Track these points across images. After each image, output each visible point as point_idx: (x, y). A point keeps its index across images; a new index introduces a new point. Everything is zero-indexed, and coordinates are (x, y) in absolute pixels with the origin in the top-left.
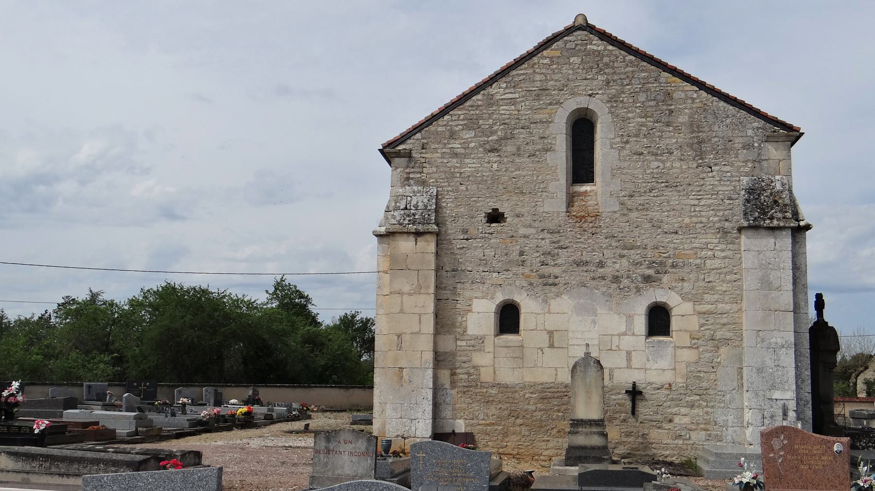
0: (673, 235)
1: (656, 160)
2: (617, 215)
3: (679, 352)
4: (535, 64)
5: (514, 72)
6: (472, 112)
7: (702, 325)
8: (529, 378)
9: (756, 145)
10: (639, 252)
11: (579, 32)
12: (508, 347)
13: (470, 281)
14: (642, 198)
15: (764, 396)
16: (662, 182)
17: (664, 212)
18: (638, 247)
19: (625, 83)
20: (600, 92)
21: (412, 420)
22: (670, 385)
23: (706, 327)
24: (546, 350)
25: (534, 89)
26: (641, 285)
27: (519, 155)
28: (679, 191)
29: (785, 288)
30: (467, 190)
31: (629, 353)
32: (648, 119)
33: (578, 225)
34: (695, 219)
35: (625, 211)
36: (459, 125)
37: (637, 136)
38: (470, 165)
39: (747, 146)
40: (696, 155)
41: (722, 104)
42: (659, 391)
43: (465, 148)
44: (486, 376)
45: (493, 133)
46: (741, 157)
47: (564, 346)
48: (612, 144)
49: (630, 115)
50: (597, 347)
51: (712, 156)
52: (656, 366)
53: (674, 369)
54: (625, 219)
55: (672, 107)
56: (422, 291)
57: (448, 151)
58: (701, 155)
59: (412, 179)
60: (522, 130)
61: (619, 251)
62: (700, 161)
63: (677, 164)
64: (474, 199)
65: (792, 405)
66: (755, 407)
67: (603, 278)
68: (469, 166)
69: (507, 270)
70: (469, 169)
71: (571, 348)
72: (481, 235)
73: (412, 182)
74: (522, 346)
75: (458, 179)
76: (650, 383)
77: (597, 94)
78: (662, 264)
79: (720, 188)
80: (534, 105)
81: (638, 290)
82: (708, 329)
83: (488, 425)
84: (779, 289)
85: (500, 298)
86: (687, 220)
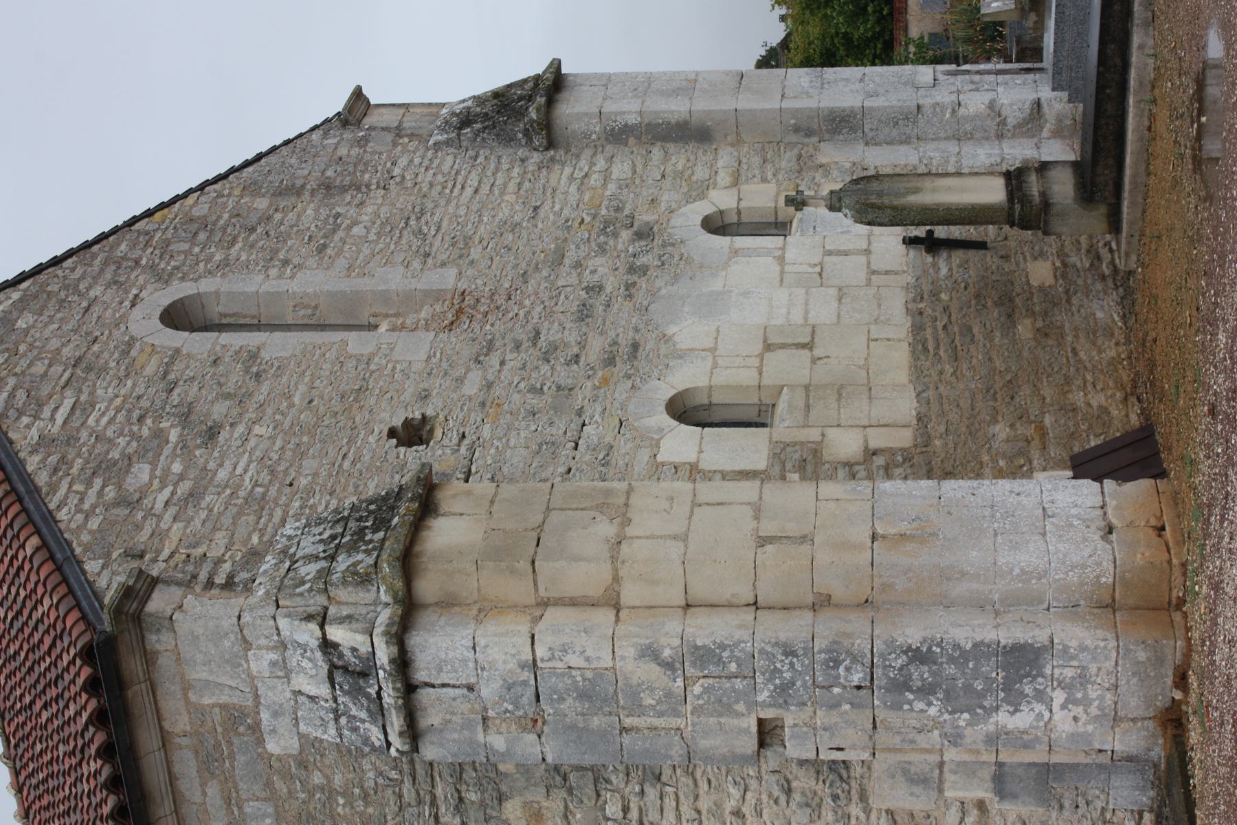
1: (349, 228)
7: (764, 180)
10: (573, 247)
12: (808, 407)
24: (818, 352)
25: (67, 375)
31: (830, 253)
34: (512, 187)
38: (239, 471)
41: (250, 169)
47: (809, 329)
57: (173, 510)
61: (564, 270)
62: (374, 187)
69: (580, 413)
70: (250, 474)
71: (811, 321)
72: (463, 450)
75: (273, 491)
78: (607, 223)
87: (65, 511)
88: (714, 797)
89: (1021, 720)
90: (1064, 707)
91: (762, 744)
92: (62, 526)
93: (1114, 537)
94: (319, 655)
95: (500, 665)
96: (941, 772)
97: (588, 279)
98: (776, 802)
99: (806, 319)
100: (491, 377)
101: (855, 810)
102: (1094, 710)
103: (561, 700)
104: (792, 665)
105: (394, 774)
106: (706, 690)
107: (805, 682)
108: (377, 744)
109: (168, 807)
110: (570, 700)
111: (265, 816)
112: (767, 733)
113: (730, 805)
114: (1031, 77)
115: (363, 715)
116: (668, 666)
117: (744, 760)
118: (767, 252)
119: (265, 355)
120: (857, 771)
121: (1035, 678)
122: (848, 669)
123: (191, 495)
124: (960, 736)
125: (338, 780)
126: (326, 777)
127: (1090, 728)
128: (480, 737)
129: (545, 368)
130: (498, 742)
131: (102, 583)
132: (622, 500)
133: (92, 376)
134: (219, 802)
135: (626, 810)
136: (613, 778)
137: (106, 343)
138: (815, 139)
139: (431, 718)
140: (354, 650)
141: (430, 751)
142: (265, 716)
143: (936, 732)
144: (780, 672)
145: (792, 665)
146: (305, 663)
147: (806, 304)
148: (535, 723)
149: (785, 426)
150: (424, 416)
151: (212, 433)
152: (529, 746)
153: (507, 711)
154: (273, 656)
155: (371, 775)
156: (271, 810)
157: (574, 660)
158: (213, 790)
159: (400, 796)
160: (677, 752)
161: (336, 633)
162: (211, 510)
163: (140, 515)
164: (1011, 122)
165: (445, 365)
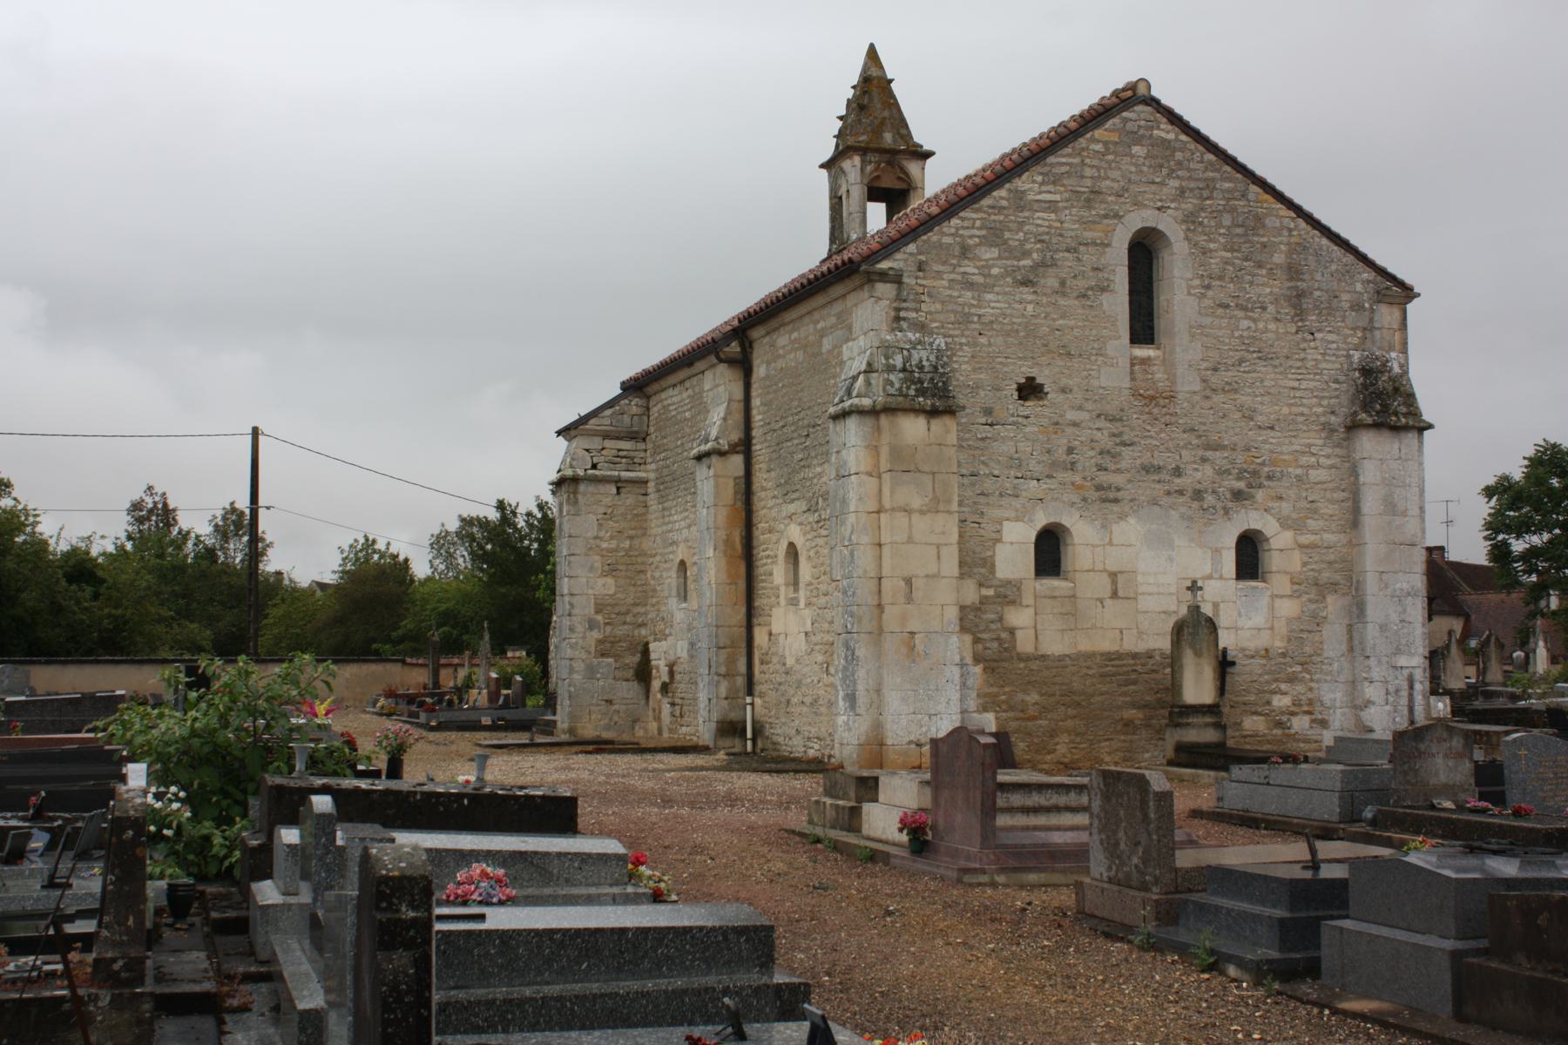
0: (1269, 431)
1: (1247, 318)
2: (1197, 398)
3: (1278, 602)
4: (1083, 149)
5: (1051, 159)
6: (993, 217)
7: (1305, 564)
8: (1085, 646)
9: (1367, 305)
10: (1226, 455)
11: (1140, 108)
12: (1055, 597)
13: (997, 493)
14: (1230, 374)
15: (1388, 663)
16: (1254, 352)
17: (1256, 396)
18: (1224, 448)
19: (1205, 196)
20: (1173, 205)
21: (930, 716)
22: (1267, 650)
23: (1310, 567)
24: (1108, 602)
25: (1083, 189)
26: (1230, 504)
27: (1064, 295)
28: (1275, 367)
29: (1410, 513)
30: (990, 345)
32: (1235, 254)
33: (1147, 410)
34: (1295, 410)
35: (1208, 393)
36: (974, 236)
37: (1221, 278)
38: (992, 305)
39: (1357, 307)
40: (1296, 315)
41: (1325, 241)
42: (1252, 660)
43: (984, 276)
44: (1025, 644)
45: (1026, 254)
46: (1349, 322)
47: (1132, 595)
48: (1190, 287)
49: (1212, 246)
50: (1175, 598)
51: (1314, 318)
52: (1250, 624)
53: (1272, 628)
54: (1207, 404)
55: (1265, 239)
56: (941, 507)
58: (1300, 314)
59: (904, 319)
60: (1066, 254)
61: (1200, 453)
62: (1300, 324)
63: (1272, 326)
64: (1000, 360)
65: (1419, 675)
66: (1377, 678)
67: (1181, 493)
68: (992, 305)
70: (991, 311)
72: (1012, 419)
73: (904, 325)
74: (1074, 596)
76: (1243, 650)
77: (1169, 207)
78: (1255, 473)
79: (1324, 365)
80: (1083, 217)
81: (1226, 511)
82: (1312, 570)
84: (1404, 513)
85: (1041, 520)
86: (1285, 410)
87: (958, 221)
92: (946, 224)
99: (1143, 594)
109: (828, 299)
131: (898, 256)
137: (1116, 203)
138: (1354, 593)
147: (1159, 594)
150: (1047, 393)
151: (1026, 283)
162: (959, 297)
163: (954, 262)
164: (1362, 714)
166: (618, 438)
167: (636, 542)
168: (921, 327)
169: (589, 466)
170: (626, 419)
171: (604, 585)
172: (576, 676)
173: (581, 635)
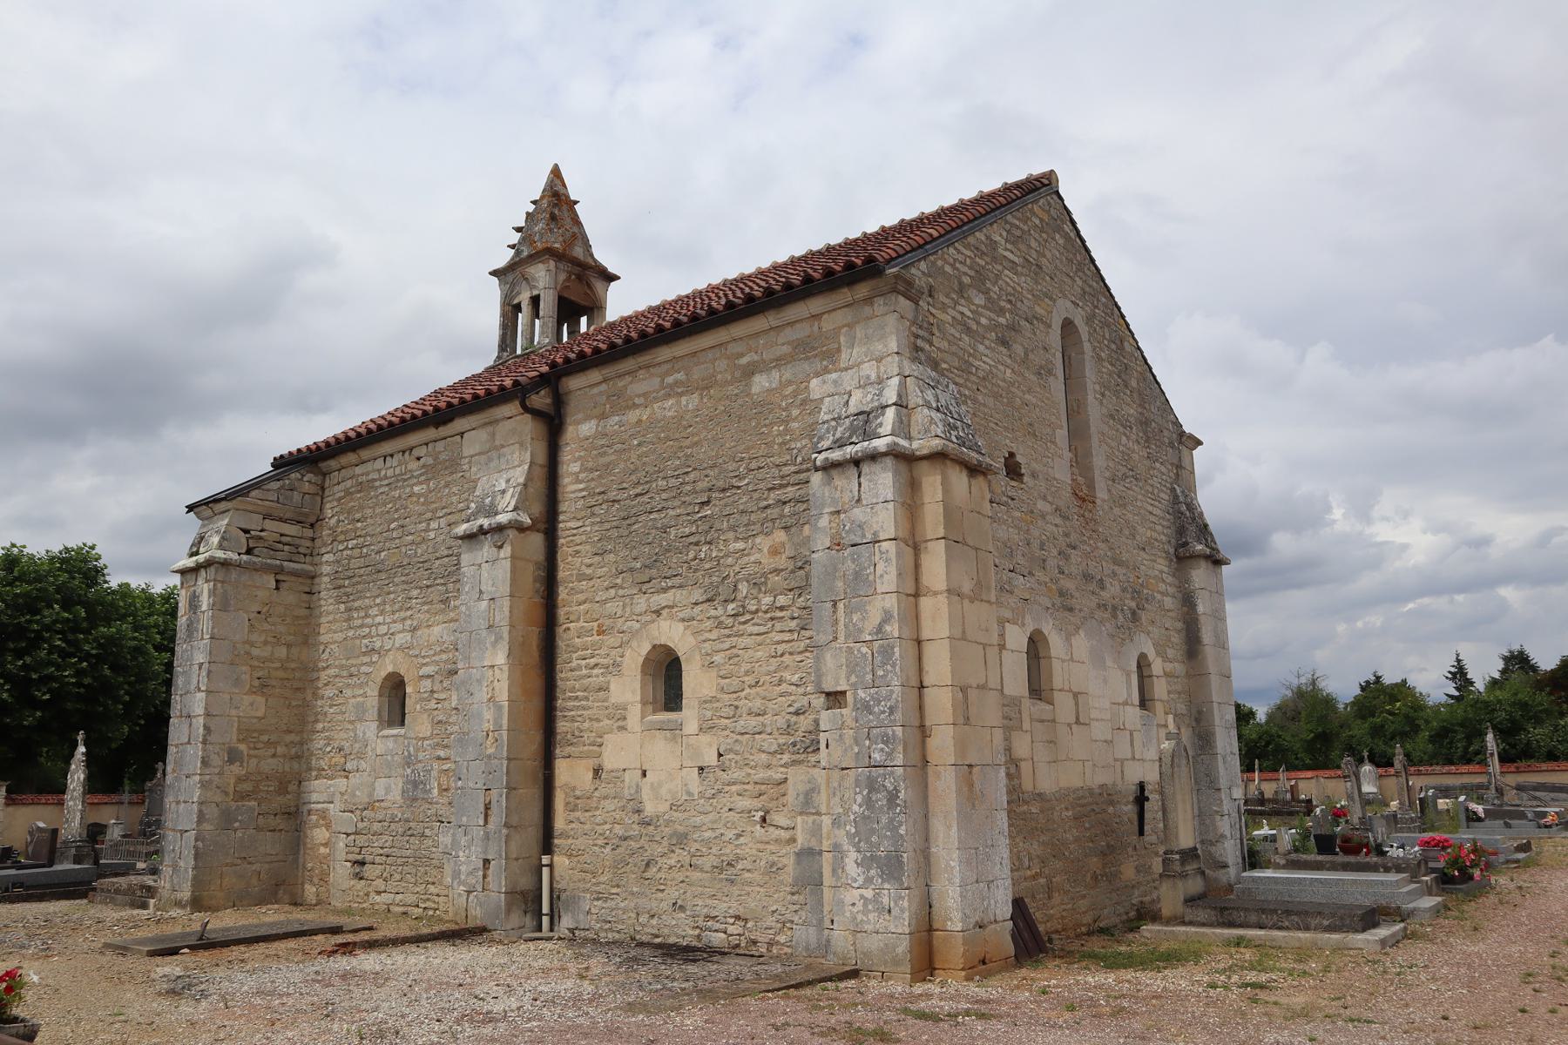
1: (1125, 434)
7: (1169, 692)
12: (1042, 721)
24: (1074, 727)
31: (1131, 735)
34: (1155, 535)
38: (984, 358)
57: (959, 317)
69: (1030, 573)
72: (1005, 499)
75: (974, 378)
83: (1034, 877)
88: (791, 664)
89: (852, 869)
90: (862, 897)
91: (828, 694)
93: (978, 930)
94: (876, 404)
95: (875, 519)
96: (813, 814)
97: (1107, 581)
98: (790, 706)
100: (1048, 517)
101: (786, 758)
102: (860, 917)
103: (853, 561)
104: (884, 712)
105: (799, 459)
106: (864, 655)
107: (871, 721)
108: (819, 445)
109: (774, 323)
110: (853, 566)
111: (771, 382)
112: (835, 698)
113: (787, 675)
114: (1240, 860)
115: (838, 435)
116: (879, 629)
117: (818, 683)
118: (1129, 695)
119: (1051, 379)
120: (813, 758)
121: (881, 877)
122: (882, 750)
123: (968, 328)
124: (838, 828)
125: (795, 425)
126: (796, 418)
127: (848, 914)
128: (827, 510)
129: (1055, 552)
130: (824, 522)
132: (984, 598)
133: (1032, 274)
134: (778, 354)
135: (782, 608)
136: (802, 599)
139: (839, 481)
140: (881, 425)
141: (817, 478)
142: (834, 376)
143: (841, 810)
144: (879, 704)
145: (884, 712)
146: (870, 396)
148: (837, 545)
149: (1030, 708)
151: (1004, 342)
152: (822, 541)
153: (845, 526)
154: (873, 377)
155: (799, 445)
156: (774, 386)
157: (880, 568)
158: (786, 349)
159: (785, 465)
160: (822, 639)
161: (890, 413)
162: (960, 340)
164: (1213, 849)
165: (1053, 489)
166: (280, 520)
167: (294, 650)
168: (935, 365)
169: (244, 551)
170: (296, 496)
171: (252, 704)
172: (206, 826)
173: (217, 771)
